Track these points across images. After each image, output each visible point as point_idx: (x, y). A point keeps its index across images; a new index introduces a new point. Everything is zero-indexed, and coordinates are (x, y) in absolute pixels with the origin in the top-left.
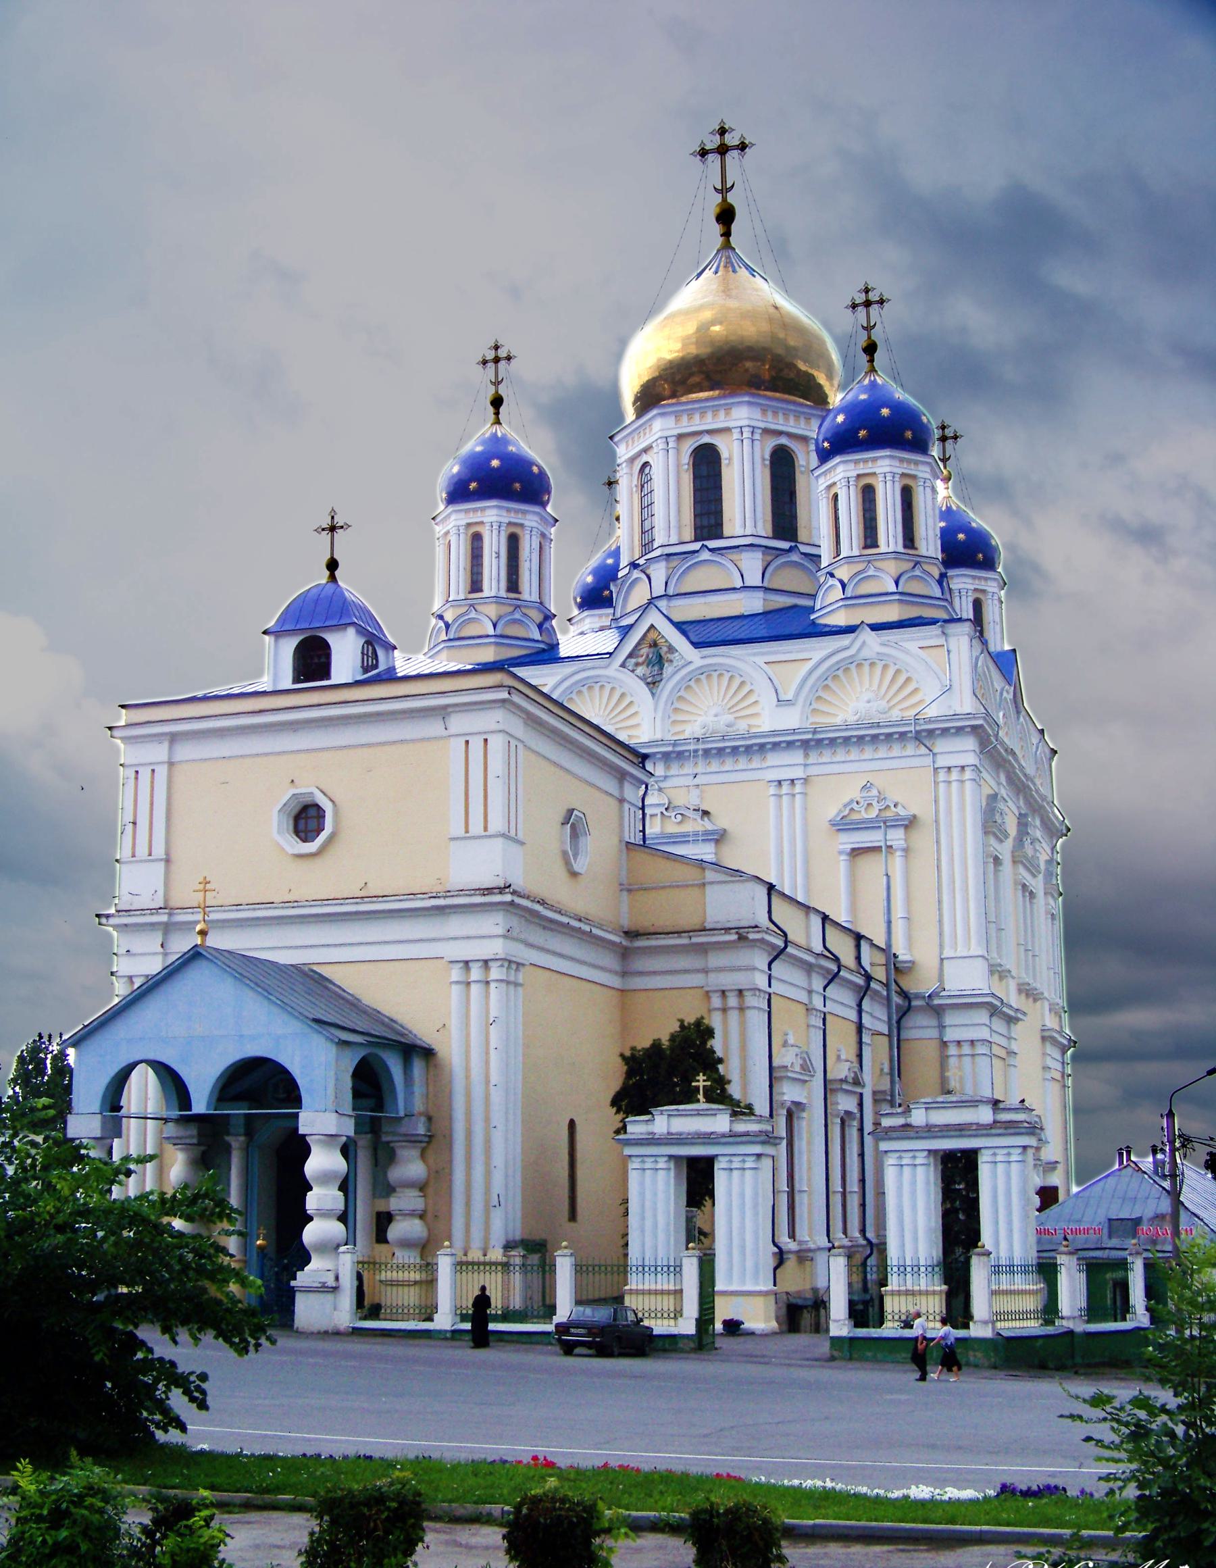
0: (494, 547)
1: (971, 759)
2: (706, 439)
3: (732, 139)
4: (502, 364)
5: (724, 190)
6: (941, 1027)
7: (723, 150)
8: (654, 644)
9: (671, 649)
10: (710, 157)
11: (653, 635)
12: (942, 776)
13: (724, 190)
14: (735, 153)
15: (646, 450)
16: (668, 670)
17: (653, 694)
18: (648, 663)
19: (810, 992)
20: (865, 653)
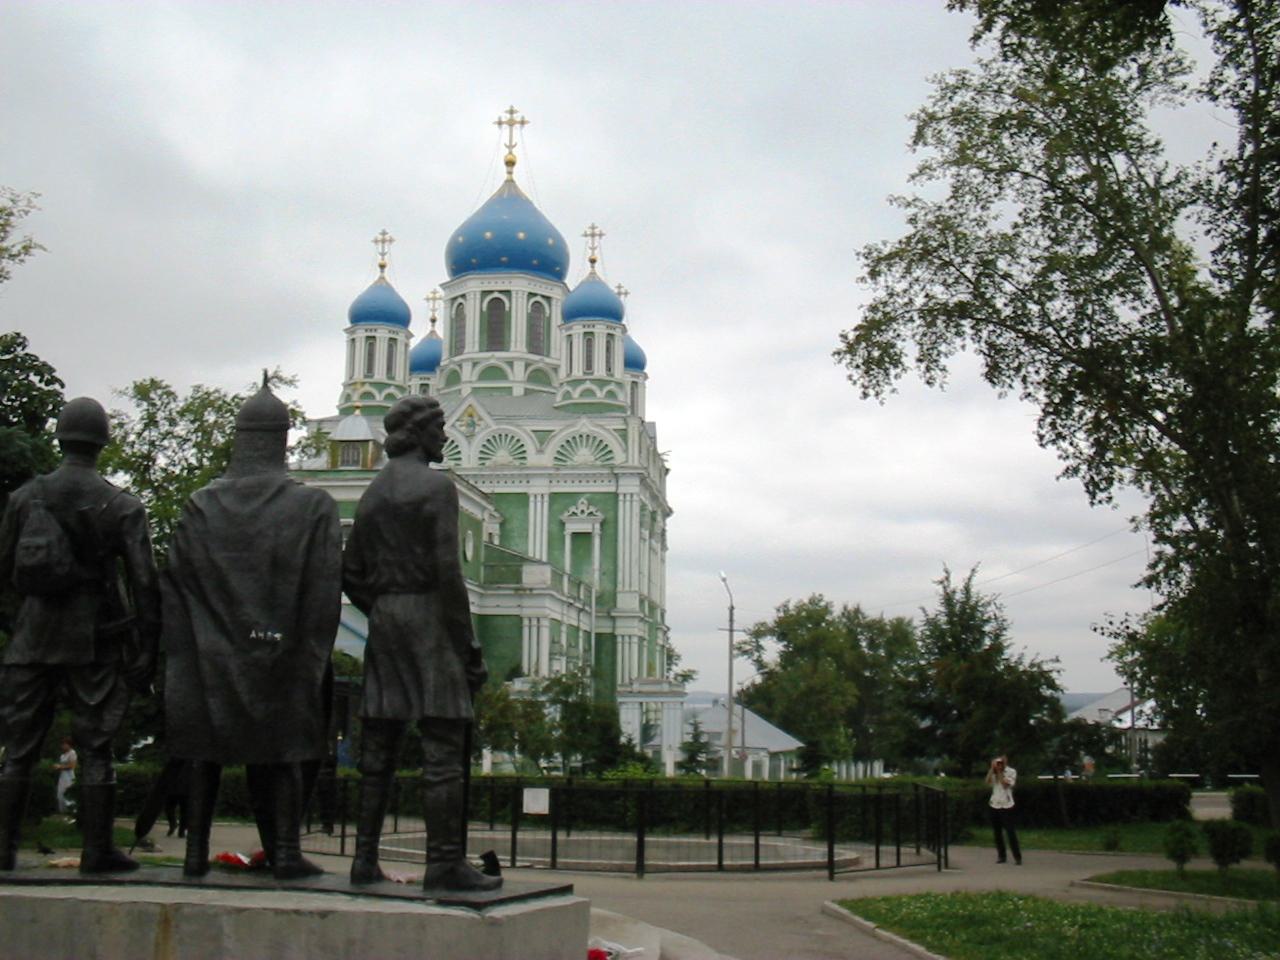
0: (381, 349)
1: (636, 490)
2: (496, 295)
3: (517, 117)
4: (387, 244)
5: (511, 147)
6: (614, 628)
7: (511, 123)
8: (471, 416)
9: (481, 419)
10: (504, 126)
11: (470, 410)
12: (621, 497)
13: (511, 147)
14: (518, 126)
15: (463, 296)
16: (477, 429)
17: (469, 443)
18: (468, 425)
19: (563, 614)
20: (585, 431)
